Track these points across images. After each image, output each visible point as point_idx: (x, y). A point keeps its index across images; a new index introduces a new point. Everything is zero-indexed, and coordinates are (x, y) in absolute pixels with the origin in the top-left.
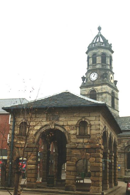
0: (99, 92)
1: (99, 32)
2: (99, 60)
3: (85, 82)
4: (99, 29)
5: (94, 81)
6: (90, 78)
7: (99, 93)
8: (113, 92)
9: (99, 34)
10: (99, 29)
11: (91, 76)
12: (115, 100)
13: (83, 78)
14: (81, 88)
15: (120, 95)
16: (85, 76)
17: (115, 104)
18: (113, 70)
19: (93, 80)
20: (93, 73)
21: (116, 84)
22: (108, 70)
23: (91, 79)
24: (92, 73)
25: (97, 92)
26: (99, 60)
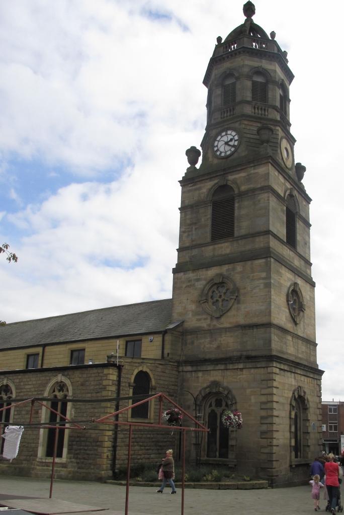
0: (243, 188)
1: (249, 20)
2: (245, 90)
3: (198, 166)
4: (249, 9)
5: (227, 157)
6: (216, 149)
7: (242, 195)
8: (291, 196)
9: (249, 23)
10: (249, 9)
11: (216, 143)
12: (299, 225)
13: (192, 154)
14: (185, 182)
15: (315, 212)
16: (200, 148)
17: (299, 238)
18: (293, 131)
19: (223, 155)
20: (224, 134)
21: (300, 177)
22: (276, 123)
23: (218, 153)
24: (222, 131)
25: (236, 191)
26: (245, 90)
